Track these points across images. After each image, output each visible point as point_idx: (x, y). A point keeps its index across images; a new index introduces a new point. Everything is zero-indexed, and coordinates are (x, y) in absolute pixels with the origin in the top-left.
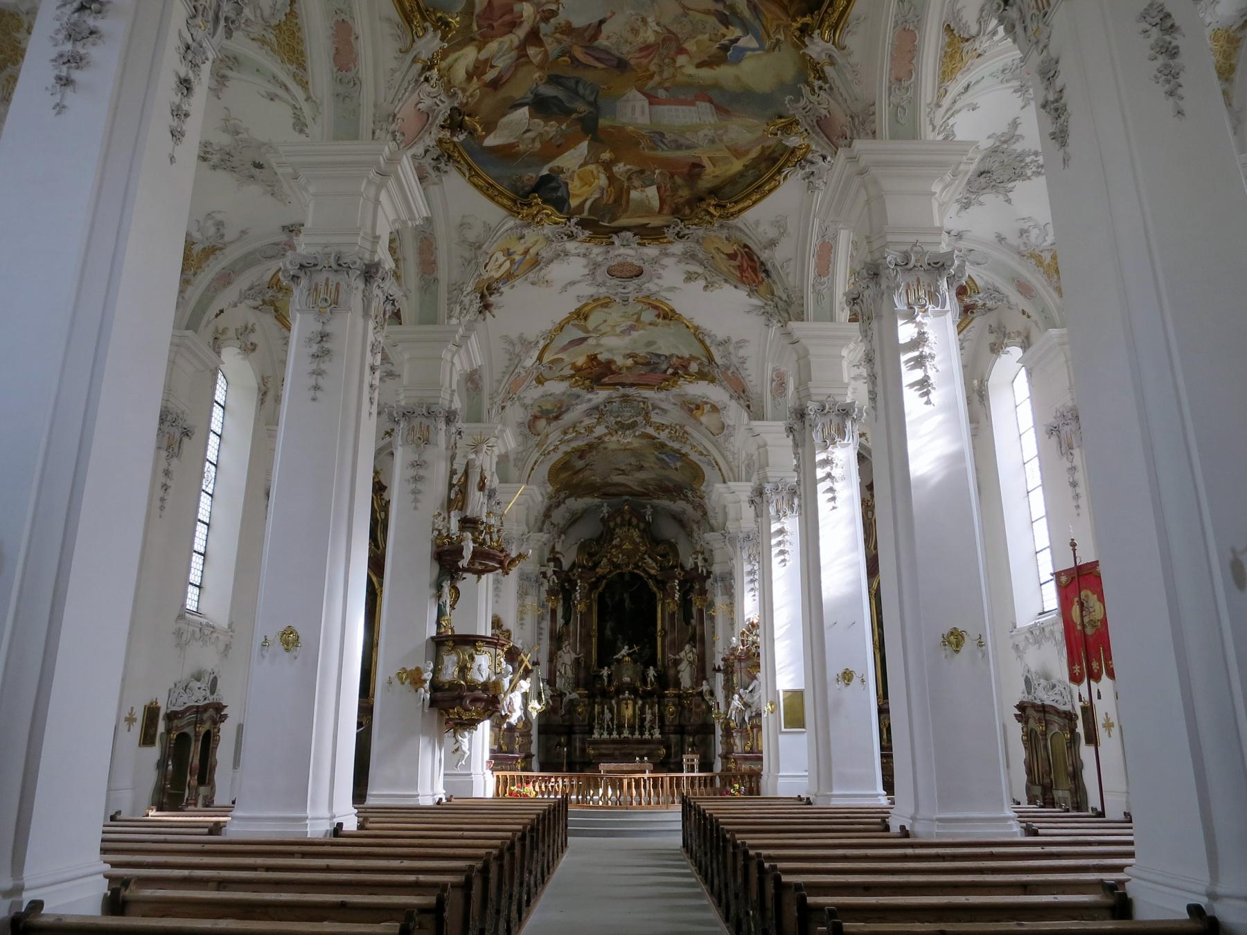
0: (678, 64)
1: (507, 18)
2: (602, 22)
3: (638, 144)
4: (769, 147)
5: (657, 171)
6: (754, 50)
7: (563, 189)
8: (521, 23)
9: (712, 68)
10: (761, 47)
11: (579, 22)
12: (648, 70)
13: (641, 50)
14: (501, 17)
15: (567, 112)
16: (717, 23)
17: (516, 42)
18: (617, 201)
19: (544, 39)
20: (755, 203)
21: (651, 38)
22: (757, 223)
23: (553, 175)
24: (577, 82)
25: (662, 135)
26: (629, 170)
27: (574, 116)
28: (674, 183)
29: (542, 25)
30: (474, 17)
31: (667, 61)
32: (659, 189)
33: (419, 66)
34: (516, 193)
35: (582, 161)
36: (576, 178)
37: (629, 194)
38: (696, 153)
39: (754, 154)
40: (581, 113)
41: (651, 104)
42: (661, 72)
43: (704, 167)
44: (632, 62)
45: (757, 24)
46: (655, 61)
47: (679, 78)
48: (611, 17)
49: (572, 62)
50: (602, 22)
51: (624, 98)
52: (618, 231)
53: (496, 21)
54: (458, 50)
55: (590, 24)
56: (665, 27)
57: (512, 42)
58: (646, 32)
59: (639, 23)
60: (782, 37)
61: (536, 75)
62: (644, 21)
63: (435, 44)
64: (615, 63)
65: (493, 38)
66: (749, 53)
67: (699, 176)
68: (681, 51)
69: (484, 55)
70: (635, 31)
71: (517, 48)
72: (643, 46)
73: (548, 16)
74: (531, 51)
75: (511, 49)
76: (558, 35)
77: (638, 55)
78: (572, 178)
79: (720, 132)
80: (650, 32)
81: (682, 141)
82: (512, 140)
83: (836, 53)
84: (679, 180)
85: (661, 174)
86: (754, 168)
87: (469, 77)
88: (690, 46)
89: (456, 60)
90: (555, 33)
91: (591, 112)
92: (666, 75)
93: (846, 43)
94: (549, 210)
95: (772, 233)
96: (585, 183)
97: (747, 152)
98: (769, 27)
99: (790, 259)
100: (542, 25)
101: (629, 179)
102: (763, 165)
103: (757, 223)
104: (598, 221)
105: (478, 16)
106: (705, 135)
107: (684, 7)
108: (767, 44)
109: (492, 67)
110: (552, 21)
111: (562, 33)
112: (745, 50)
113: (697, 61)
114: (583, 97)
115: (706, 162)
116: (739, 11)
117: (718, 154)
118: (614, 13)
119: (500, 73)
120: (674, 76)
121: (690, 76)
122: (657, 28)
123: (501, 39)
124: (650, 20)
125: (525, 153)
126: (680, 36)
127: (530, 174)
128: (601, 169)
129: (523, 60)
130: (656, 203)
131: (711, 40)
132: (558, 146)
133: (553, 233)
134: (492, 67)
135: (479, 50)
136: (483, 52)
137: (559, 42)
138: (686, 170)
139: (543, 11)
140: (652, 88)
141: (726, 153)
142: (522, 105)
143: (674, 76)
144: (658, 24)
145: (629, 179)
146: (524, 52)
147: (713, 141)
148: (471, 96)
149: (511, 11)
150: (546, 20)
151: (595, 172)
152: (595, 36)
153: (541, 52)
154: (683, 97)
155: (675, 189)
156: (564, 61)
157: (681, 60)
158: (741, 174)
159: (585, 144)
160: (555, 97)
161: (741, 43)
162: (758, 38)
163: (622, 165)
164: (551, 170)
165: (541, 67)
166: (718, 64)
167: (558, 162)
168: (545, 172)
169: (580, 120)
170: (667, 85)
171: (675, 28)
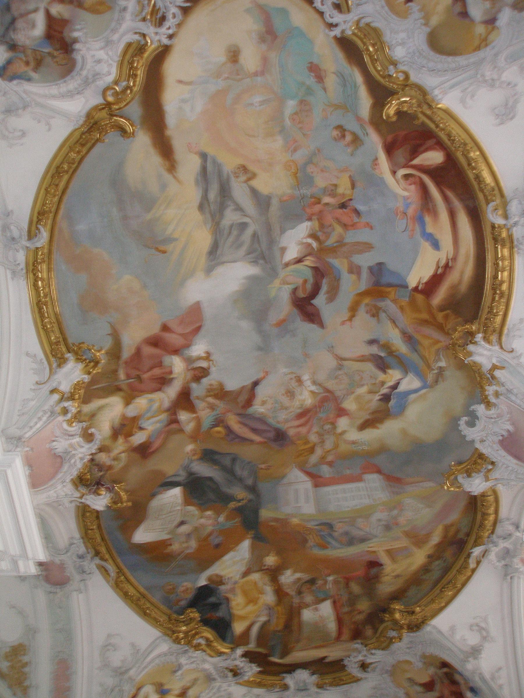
0: (339, 430)
1: (157, 372)
2: (256, 384)
3: (306, 541)
4: (452, 525)
5: (330, 578)
6: (416, 391)
7: (223, 607)
8: (172, 379)
9: (378, 428)
12: (307, 442)
13: (300, 416)
14: (151, 368)
15: (227, 499)
17: (167, 404)
18: (288, 626)
20: (448, 604)
22: (453, 629)
23: (212, 586)
24: (234, 460)
25: (330, 526)
26: (299, 579)
27: (232, 505)
28: (350, 593)
29: (194, 385)
30: (121, 362)
31: (328, 427)
32: (334, 603)
33: (56, 397)
34: (170, 608)
35: (243, 569)
36: (238, 591)
37: (299, 614)
38: (372, 546)
39: (436, 539)
40: (239, 501)
41: (316, 485)
42: (323, 442)
43: (381, 565)
44: (291, 432)
45: (415, 357)
46: (315, 429)
47: (343, 448)
48: (264, 378)
49: (227, 435)
50: (256, 384)
51: (285, 481)
52: (291, 668)
53: (145, 372)
54: (103, 397)
55: (243, 387)
56: (320, 385)
58: (301, 394)
59: (294, 384)
61: (190, 447)
62: (299, 381)
63: (76, 374)
64: (272, 435)
65: (142, 392)
66: (413, 396)
67: (377, 578)
68: (342, 412)
69: (131, 411)
70: (290, 394)
71: (168, 410)
72: (299, 411)
74: (183, 416)
75: (160, 411)
76: (211, 400)
77: (297, 423)
78: (233, 590)
79: (395, 512)
81: (356, 533)
82: (164, 536)
83: (506, 356)
84: (356, 588)
85: (335, 582)
86: (438, 558)
87: (116, 433)
88: (350, 405)
89: (101, 408)
90: (207, 396)
91: (250, 501)
92: (329, 445)
93: (514, 346)
94: (208, 633)
95: (473, 639)
96: (251, 601)
97: (428, 537)
98: (427, 354)
99: (500, 669)
100: (194, 385)
101: (299, 593)
102: (448, 554)
103: (453, 629)
104: (266, 656)
105: (126, 363)
106: (379, 520)
108: (430, 378)
109: (141, 429)
110: (205, 381)
113: (360, 421)
114: (241, 480)
115: (384, 559)
117: (397, 545)
118: (267, 373)
119: (149, 437)
120: (336, 446)
121: (354, 443)
122: (313, 388)
124: (306, 377)
125: (179, 555)
126: (338, 393)
127: (185, 584)
128: (267, 579)
129: (174, 426)
130: (332, 626)
131: (371, 392)
132: (217, 546)
133: (216, 668)
134: (141, 429)
135: (128, 402)
136: (131, 407)
137: (212, 407)
138: (360, 572)
139: (194, 369)
140: (315, 465)
141: (404, 542)
142: (173, 484)
143: (336, 446)
144: (314, 383)
145: (299, 593)
146: (174, 417)
147: (388, 528)
148: (115, 459)
149: (160, 364)
150: (197, 379)
151: (260, 584)
152: (249, 402)
153: (194, 418)
154: (348, 472)
155: (353, 600)
156: (219, 432)
157: (343, 423)
158: (425, 569)
159: (246, 545)
160: (210, 479)
161: (402, 388)
163: (288, 572)
164: (210, 579)
165: (195, 437)
167: (216, 569)
168: (202, 582)
169: (240, 510)
170: (330, 458)
171: (331, 385)
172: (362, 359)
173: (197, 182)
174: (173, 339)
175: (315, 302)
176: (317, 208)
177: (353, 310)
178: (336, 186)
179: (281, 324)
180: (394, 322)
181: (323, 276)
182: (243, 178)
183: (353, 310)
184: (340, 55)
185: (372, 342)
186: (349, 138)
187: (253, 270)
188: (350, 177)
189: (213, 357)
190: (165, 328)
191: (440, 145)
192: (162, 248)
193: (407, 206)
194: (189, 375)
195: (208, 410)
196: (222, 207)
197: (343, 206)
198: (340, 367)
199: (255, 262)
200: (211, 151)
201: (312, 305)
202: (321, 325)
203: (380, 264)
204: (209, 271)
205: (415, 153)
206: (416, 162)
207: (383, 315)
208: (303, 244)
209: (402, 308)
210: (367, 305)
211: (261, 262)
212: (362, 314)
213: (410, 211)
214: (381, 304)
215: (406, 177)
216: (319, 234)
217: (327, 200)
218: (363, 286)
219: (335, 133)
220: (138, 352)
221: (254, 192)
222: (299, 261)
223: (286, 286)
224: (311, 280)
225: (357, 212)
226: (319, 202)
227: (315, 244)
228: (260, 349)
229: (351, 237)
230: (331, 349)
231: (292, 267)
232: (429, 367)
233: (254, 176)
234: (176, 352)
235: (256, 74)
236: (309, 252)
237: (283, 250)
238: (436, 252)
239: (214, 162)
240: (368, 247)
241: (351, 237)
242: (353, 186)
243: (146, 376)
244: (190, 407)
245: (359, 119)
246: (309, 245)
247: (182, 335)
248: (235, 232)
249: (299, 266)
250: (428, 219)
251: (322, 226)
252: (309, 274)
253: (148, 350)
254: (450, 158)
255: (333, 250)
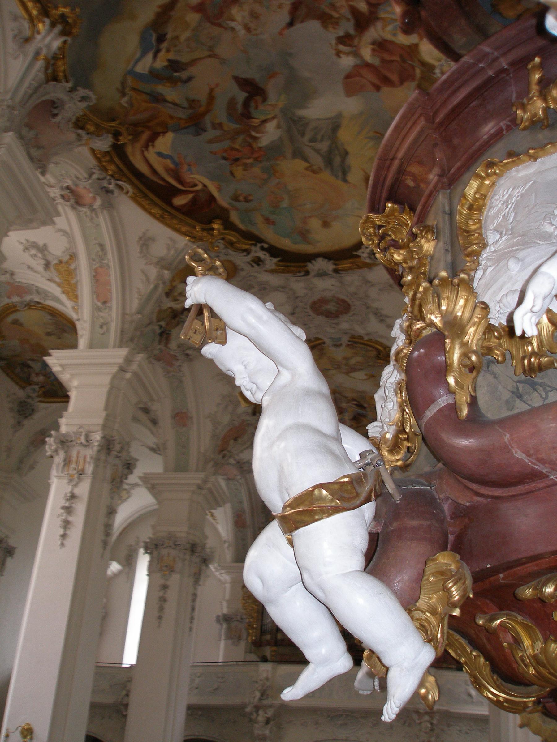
2: (291, 24)
9: (160, 6)
10: (131, 72)
11: (314, 25)
16: (178, 58)
17: (379, 25)
19: (350, 16)
21: (235, 11)
29: (352, 32)
48: (283, 29)
50: (291, 24)
55: (302, 22)
56: (226, 29)
57: (383, 29)
59: (252, 25)
60: (124, 101)
62: (248, 29)
66: (138, 54)
70: (254, 16)
71: (377, 19)
73: (345, 40)
76: (335, 15)
80: (239, 18)
88: (193, 18)
90: (338, 18)
100: (352, 32)
107: (214, 56)
108: (130, 81)
110: (341, 33)
111: (330, 17)
112: (144, 54)
116: (168, 84)
118: (281, 34)
122: (233, 24)
123: (393, 39)
124: (242, 32)
126: (207, 25)
131: (177, 38)
144: (233, 29)
149: (383, 61)
161: (150, 56)
162: (139, 77)
166: (159, 15)
171: (216, 31)
172: (193, 63)
173: (349, 167)
174: (371, 77)
175: (245, 95)
176: (256, 155)
177: (211, 98)
178: (245, 170)
179: (273, 75)
180: (175, 104)
181: (242, 115)
182: (315, 167)
183: (211, 98)
184: (256, 232)
185: (189, 79)
186: (241, 198)
187: (301, 113)
188: (234, 177)
189: (334, 52)
190: (378, 88)
191: (178, 209)
192: (378, 135)
193: (190, 170)
194: (356, 41)
195: (338, 5)
196: (330, 151)
197: (237, 160)
198: (211, 49)
199: (301, 118)
200: (339, 182)
201: (248, 92)
202: (237, 79)
203: (198, 134)
204: (339, 116)
205: (194, 201)
206: (191, 196)
207: (185, 104)
208: (263, 133)
209: (171, 117)
210: (200, 106)
211: (296, 119)
212: (203, 98)
213: (185, 167)
214: (190, 112)
215: (195, 185)
216: (251, 141)
217: (250, 161)
218: (208, 119)
219: (251, 198)
220: (402, 82)
221: (306, 160)
222: (264, 121)
223: (274, 103)
224: (252, 110)
225: (225, 158)
226: (256, 159)
227: (253, 134)
228: (290, 55)
229: (227, 144)
230: (223, 61)
231: (270, 116)
232: (133, 89)
233: (307, 169)
234: (368, 65)
235: (310, 217)
236: (256, 129)
237: (278, 127)
238: (158, 151)
239: (337, 177)
240: (210, 142)
241: (227, 144)
242: (232, 173)
243: (397, 58)
244: (355, 12)
245: (237, 209)
246: (257, 133)
247: (361, 76)
248: (319, 137)
249: (263, 118)
250: (171, 166)
251: (250, 146)
252: (254, 113)
253: (394, 78)
254: (170, 204)
255: (238, 133)
